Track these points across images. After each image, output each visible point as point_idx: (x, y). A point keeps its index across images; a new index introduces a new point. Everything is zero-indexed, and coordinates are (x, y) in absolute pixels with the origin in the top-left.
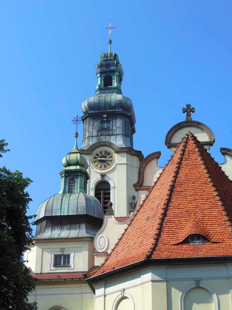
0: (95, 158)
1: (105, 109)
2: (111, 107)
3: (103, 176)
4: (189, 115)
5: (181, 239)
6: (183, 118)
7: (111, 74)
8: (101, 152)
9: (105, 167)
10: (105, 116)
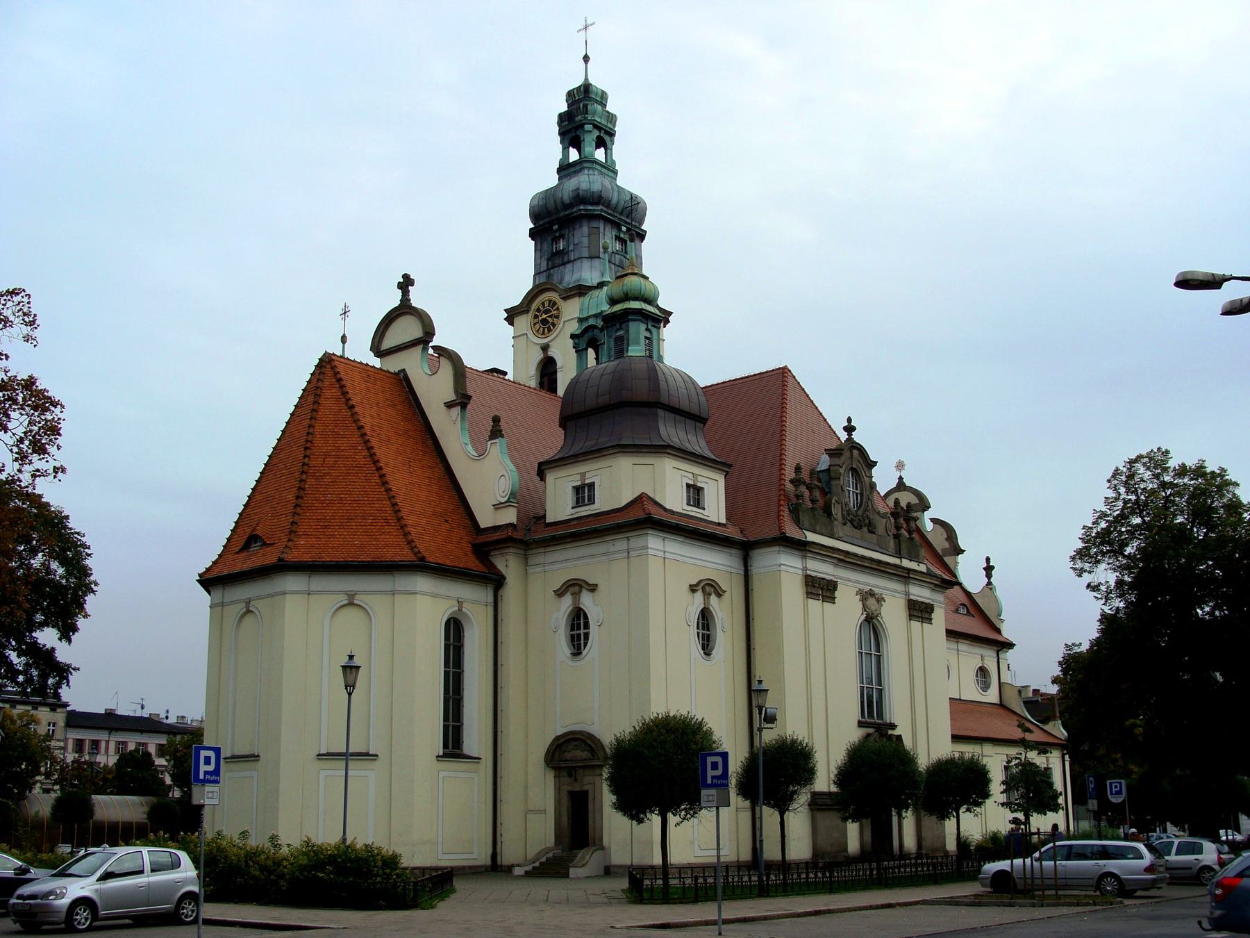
0: (536, 317)
1: (557, 210)
2: (571, 205)
3: (545, 348)
4: (405, 293)
6: (395, 299)
7: (578, 132)
8: (543, 304)
9: (550, 330)
10: (556, 227)
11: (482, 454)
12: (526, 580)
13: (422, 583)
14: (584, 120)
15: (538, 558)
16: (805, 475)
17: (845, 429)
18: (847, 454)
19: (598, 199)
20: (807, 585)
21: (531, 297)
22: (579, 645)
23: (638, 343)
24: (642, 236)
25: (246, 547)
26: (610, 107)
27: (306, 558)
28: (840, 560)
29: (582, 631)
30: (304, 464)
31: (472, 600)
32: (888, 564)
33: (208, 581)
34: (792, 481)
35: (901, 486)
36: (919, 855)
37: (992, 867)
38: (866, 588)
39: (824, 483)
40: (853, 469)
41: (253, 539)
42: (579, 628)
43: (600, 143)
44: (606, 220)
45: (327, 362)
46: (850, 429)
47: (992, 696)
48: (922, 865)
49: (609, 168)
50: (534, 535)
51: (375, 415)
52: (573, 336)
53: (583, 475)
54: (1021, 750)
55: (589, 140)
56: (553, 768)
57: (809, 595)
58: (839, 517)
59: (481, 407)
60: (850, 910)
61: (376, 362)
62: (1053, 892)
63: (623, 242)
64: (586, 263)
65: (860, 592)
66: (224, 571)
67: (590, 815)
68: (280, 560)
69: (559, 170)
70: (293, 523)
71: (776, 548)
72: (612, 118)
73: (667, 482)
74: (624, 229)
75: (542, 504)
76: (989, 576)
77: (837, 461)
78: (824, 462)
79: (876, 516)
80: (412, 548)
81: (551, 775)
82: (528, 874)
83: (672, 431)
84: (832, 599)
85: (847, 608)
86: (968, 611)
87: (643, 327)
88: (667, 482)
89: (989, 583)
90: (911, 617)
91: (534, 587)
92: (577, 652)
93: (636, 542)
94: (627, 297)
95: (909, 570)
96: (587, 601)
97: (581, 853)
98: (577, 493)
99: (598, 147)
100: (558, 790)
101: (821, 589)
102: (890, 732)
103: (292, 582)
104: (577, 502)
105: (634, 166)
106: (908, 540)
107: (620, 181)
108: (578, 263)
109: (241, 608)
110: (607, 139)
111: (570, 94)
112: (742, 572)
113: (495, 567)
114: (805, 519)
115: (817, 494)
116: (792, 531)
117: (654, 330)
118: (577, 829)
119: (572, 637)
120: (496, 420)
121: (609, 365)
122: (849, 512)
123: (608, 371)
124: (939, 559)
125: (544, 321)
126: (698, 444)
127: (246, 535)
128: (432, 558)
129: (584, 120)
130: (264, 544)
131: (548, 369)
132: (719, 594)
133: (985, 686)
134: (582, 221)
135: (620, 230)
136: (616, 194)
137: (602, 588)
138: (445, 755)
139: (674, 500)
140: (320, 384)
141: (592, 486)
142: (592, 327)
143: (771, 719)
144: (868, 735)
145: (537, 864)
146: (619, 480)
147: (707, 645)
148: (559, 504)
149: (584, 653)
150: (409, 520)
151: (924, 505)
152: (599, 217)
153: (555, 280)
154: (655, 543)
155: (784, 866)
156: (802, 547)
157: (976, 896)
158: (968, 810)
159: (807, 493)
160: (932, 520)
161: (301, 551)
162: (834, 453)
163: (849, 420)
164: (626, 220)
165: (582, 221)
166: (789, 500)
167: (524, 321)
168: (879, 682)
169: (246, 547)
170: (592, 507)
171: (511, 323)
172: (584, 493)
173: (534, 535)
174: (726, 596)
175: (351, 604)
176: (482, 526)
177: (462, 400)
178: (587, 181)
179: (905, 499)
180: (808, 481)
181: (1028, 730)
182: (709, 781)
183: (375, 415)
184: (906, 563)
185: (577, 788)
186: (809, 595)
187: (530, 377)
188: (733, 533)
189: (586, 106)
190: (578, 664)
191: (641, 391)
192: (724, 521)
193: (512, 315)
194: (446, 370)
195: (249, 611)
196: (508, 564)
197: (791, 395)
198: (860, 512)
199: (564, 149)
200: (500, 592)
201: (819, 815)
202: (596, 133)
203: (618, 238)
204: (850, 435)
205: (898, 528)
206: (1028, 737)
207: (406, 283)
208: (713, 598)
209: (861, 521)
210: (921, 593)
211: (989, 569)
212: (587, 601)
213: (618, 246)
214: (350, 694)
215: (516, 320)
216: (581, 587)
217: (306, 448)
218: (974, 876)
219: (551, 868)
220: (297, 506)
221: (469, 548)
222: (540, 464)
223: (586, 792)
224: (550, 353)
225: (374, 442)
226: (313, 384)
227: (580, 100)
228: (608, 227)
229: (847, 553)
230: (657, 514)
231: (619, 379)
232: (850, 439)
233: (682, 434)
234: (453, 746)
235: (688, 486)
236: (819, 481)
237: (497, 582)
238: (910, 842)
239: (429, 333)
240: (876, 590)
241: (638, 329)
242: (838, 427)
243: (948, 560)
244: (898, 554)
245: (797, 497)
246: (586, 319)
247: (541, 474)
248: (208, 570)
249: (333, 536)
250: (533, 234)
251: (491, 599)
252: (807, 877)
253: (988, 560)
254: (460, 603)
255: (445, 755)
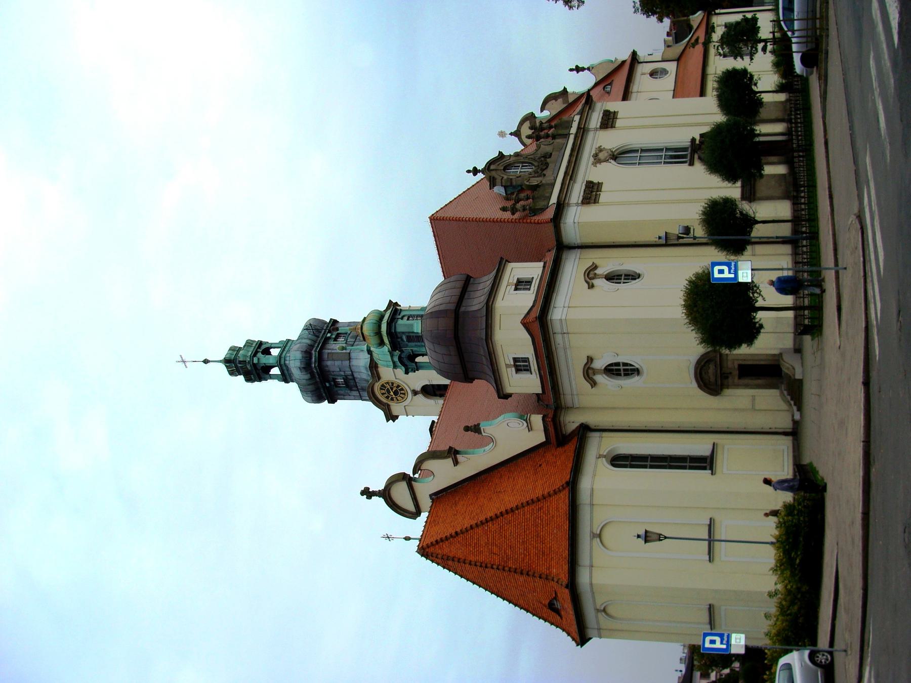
0: (392, 399)
3: (415, 393)
5: (559, 618)
6: (379, 501)
8: (383, 394)
9: (402, 389)
10: (327, 385)
11: (491, 440)
12: (583, 408)
13: (585, 484)
14: (250, 364)
15: (567, 399)
16: (509, 204)
17: (475, 174)
18: (493, 174)
19: (307, 354)
20: (589, 203)
21: (378, 403)
22: (632, 370)
23: (412, 325)
24: (334, 322)
25: (557, 611)
26: (241, 344)
27: (566, 567)
28: (571, 179)
29: (621, 367)
30: (498, 568)
31: (598, 447)
32: (574, 144)
33: (582, 639)
34: (513, 214)
35: (517, 134)
36: (789, 121)
37: (798, 67)
38: (592, 159)
39: (514, 190)
40: (505, 169)
41: (551, 606)
42: (619, 370)
43: (267, 352)
44: (323, 348)
45: (425, 551)
46: (475, 171)
47: (672, 67)
48: (796, 118)
49: (285, 345)
50: (550, 402)
51: (462, 517)
52: (407, 373)
53: (507, 366)
54: (712, 45)
55: (264, 360)
56: (721, 390)
57: (596, 201)
58: (540, 179)
59: (457, 439)
60: (829, 172)
61: (424, 516)
62: (818, 21)
63: (338, 336)
64: (354, 362)
65: (594, 164)
66: (574, 628)
67: (757, 363)
68: (567, 587)
69: (286, 381)
70: (540, 577)
71: (562, 225)
72: (249, 343)
73: (512, 305)
74: (329, 335)
75: (528, 396)
76: (583, 69)
77: (498, 181)
78: (499, 190)
79: (539, 152)
80: (560, 491)
81: (727, 392)
82: (800, 409)
83: (476, 301)
84: (599, 185)
85: (607, 174)
86: (610, 84)
87: (400, 322)
88: (512, 305)
89: (588, 69)
90: (613, 127)
91: (590, 403)
92: (637, 371)
93: (557, 327)
94: (378, 333)
95: (579, 128)
96: (599, 364)
97: (784, 370)
98: (521, 370)
99: (269, 353)
100: (737, 386)
101: (592, 193)
102: (697, 142)
103: (584, 578)
104: (527, 370)
105: (284, 327)
106: (556, 129)
107: (294, 337)
108: (354, 369)
109: (602, 616)
110: (263, 347)
111: (232, 373)
112: (579, 250)
113: (574, 431)
114: (541, 204)
115: (522, 195)
116: (550, 214)
117: (403, 314)
118: (767, 373)
119: (626, 375)
120: (467, 429)
121: (428, 346)
122: (536, 172)
123: (432, 347)
124: (571, 106)
125: (396, 393)
126: (486, 282)
127: (549, 611)
128: (567, 477)
129: (250, 364)
130: (556, 598)
131: (430, 391)
132: (595, 267)
133: (664, 72)
134: (323, 365)
135: (330, 338)
136: (304, 341)
137: (590, 353)
138: (711, 469)
139: (526, 300)
140: (439, 556)
141: (515, 360)
142: (400, 358)
143: (687, 230)
144: (700, 158)
145: (792, 403)
146: (511, 339)
147: (633, 276)
148: (527, 384)
149: (637, 366)
150: (539, 493)
151: (531, 117)
152: (320, 353)
153: (365, 385)
154: (557, 314)
155: (796, 221)
156: (561, 207)
157: (820, 79)
158: (756, 85)
159: (522, 203)
160: (542, 111)
161: (561, 571)
162: (493, 182)
163: (469, 171)
164: (322, 333)
165: (323, 365)
166: (526, 216)
167: (395, 408)
168: (661, 150)
169: (557, 611)
170: (531, 360)
171: (397, 417)
172: (520, 365)
173: (550, 402)
174: (597, 262)
175: (600, 536)
176: (544, 439)
177: (453, 454)
178: (295, 361)
179: (526, 131)
180: (513, 202)
181: (697, 40)
182: (732, 276)
183: (462, 517)
184: (573, 130)
185: (736, 373)
186: (596, 201)
187: (437, 403)
188: (550, 257)
189: (240, 362)
190: (645, 371)
191: (446, 324)
192: (542, 264)
193: (391, 417)
194: (429, 465)
195: (604, 610)
196: (572, 421)
197: (450, 214)
198: (536, 164)
199: (271, 378)
200: (593, 427)
201: (758, 195)
202: (260, 355)
203: (335, 340)
204: (479, 171)
205: (547, 136)
206: (702, 40)
207: (367, 493)
208: (598, 272)
209: (542, 163)
210: (595, 119)
211: (578, 69)
212: (599, 364)
213: (341, 339)
214: (666, 538)
215: (395, 413)
216: (589, 368)
217: (486, 567)
218: (804, 80)
219: (795, 392)
220: (528, 574)
221: (560, 450)
222: (499, 397)
223: (740, 366)
224: (418, 388)
225: (482, 518)
226: (440, 561)
227: (236, 366)
228: (328, 346)
229: (566, 173)
230: (537, 312)
231: (438, 339)
232: (483, 171)
233: (478, 294)
234: (704, 463)
235: (516, 289)
236: (512, 193)
237: (585, 430)
238: (779, 128)
239: (403, 477)
240: (593, 152)
241: (402, 325)
242: (473, 180)
243: (571, 100)
244: (567, 136)
245: (524, 210)
246: (394, 363)
247: (507, 396)
248: (573, 639)
249: (550, 548)
250: (332, 401)
251: (597, 434)
252: (804, 204)
253: (571, 70)
254: (600, 456)
255: (711, 469)
